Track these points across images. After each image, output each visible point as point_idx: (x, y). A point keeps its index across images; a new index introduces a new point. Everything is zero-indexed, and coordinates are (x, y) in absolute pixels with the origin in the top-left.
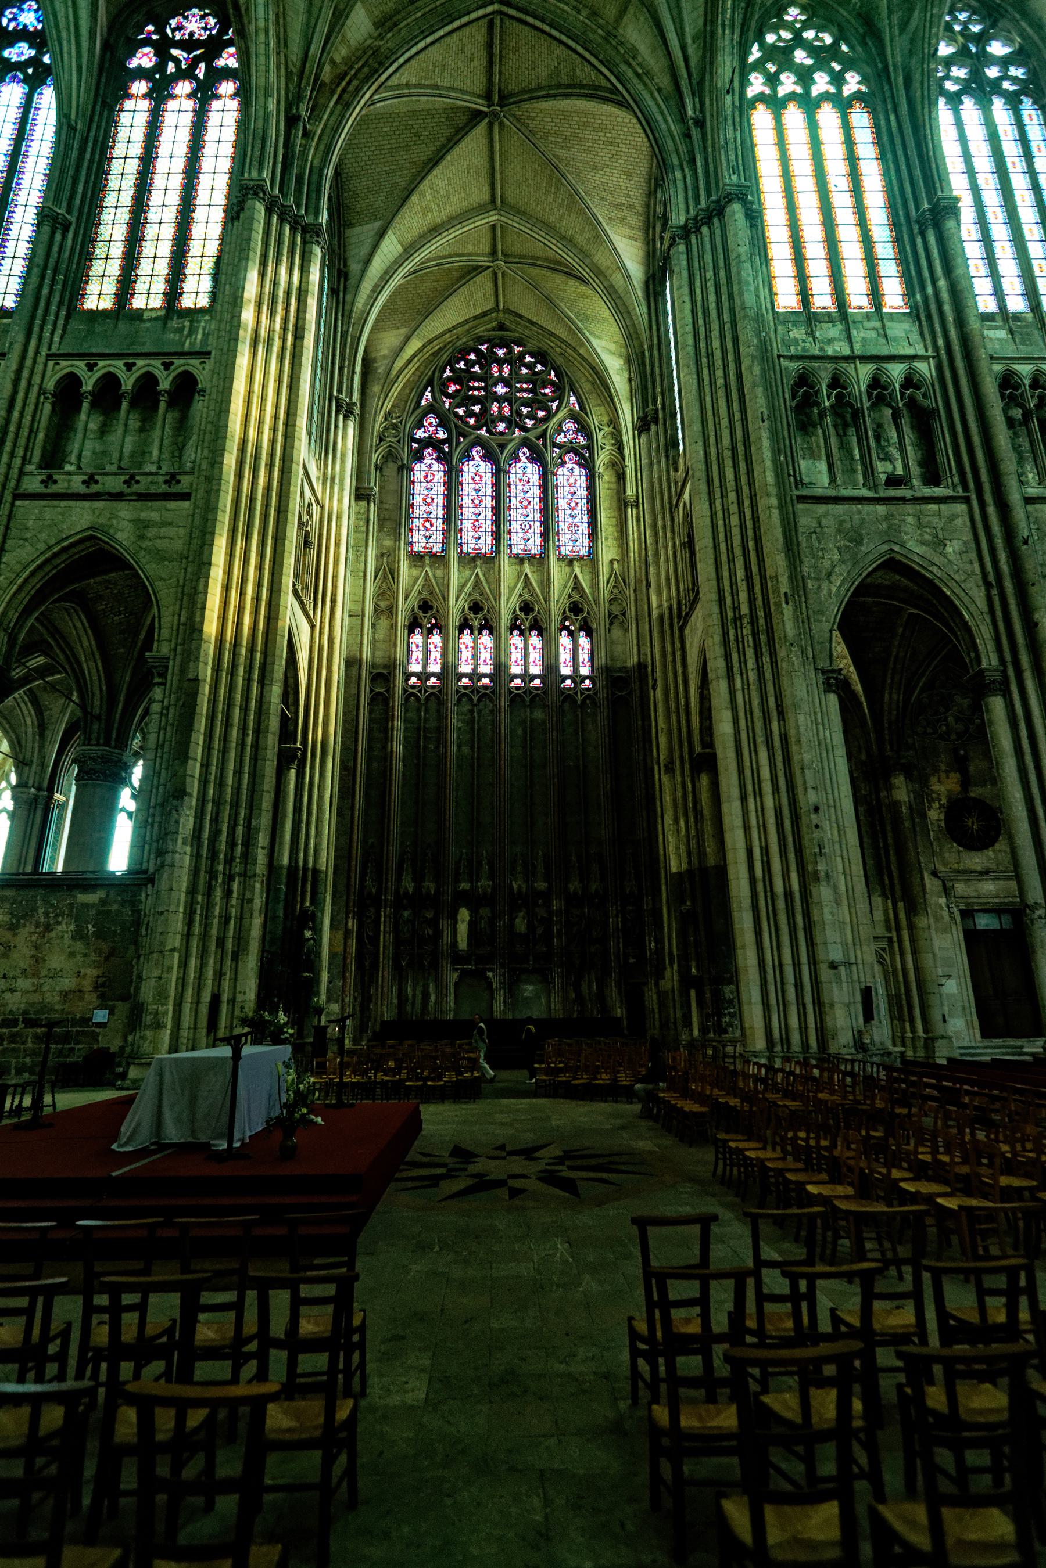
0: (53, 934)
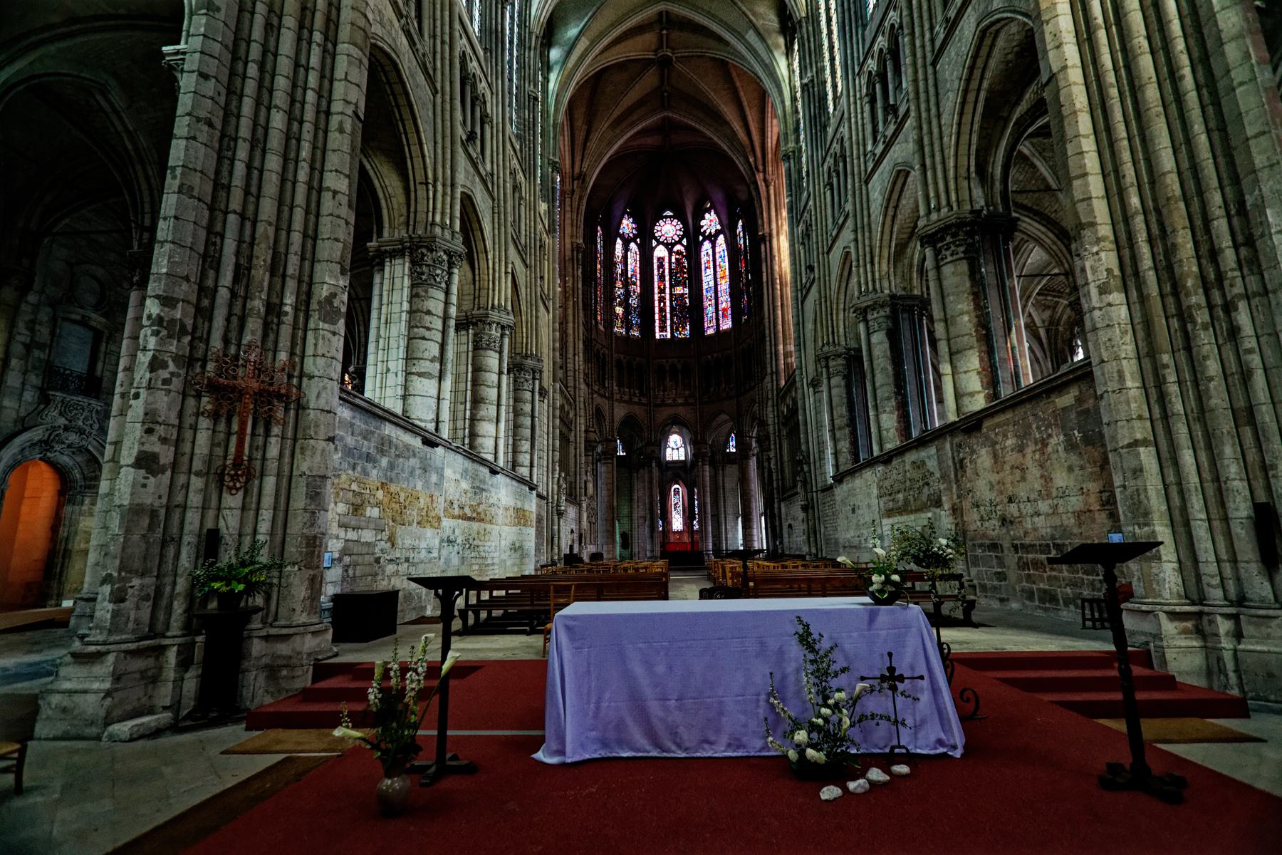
0: (1049, 449)
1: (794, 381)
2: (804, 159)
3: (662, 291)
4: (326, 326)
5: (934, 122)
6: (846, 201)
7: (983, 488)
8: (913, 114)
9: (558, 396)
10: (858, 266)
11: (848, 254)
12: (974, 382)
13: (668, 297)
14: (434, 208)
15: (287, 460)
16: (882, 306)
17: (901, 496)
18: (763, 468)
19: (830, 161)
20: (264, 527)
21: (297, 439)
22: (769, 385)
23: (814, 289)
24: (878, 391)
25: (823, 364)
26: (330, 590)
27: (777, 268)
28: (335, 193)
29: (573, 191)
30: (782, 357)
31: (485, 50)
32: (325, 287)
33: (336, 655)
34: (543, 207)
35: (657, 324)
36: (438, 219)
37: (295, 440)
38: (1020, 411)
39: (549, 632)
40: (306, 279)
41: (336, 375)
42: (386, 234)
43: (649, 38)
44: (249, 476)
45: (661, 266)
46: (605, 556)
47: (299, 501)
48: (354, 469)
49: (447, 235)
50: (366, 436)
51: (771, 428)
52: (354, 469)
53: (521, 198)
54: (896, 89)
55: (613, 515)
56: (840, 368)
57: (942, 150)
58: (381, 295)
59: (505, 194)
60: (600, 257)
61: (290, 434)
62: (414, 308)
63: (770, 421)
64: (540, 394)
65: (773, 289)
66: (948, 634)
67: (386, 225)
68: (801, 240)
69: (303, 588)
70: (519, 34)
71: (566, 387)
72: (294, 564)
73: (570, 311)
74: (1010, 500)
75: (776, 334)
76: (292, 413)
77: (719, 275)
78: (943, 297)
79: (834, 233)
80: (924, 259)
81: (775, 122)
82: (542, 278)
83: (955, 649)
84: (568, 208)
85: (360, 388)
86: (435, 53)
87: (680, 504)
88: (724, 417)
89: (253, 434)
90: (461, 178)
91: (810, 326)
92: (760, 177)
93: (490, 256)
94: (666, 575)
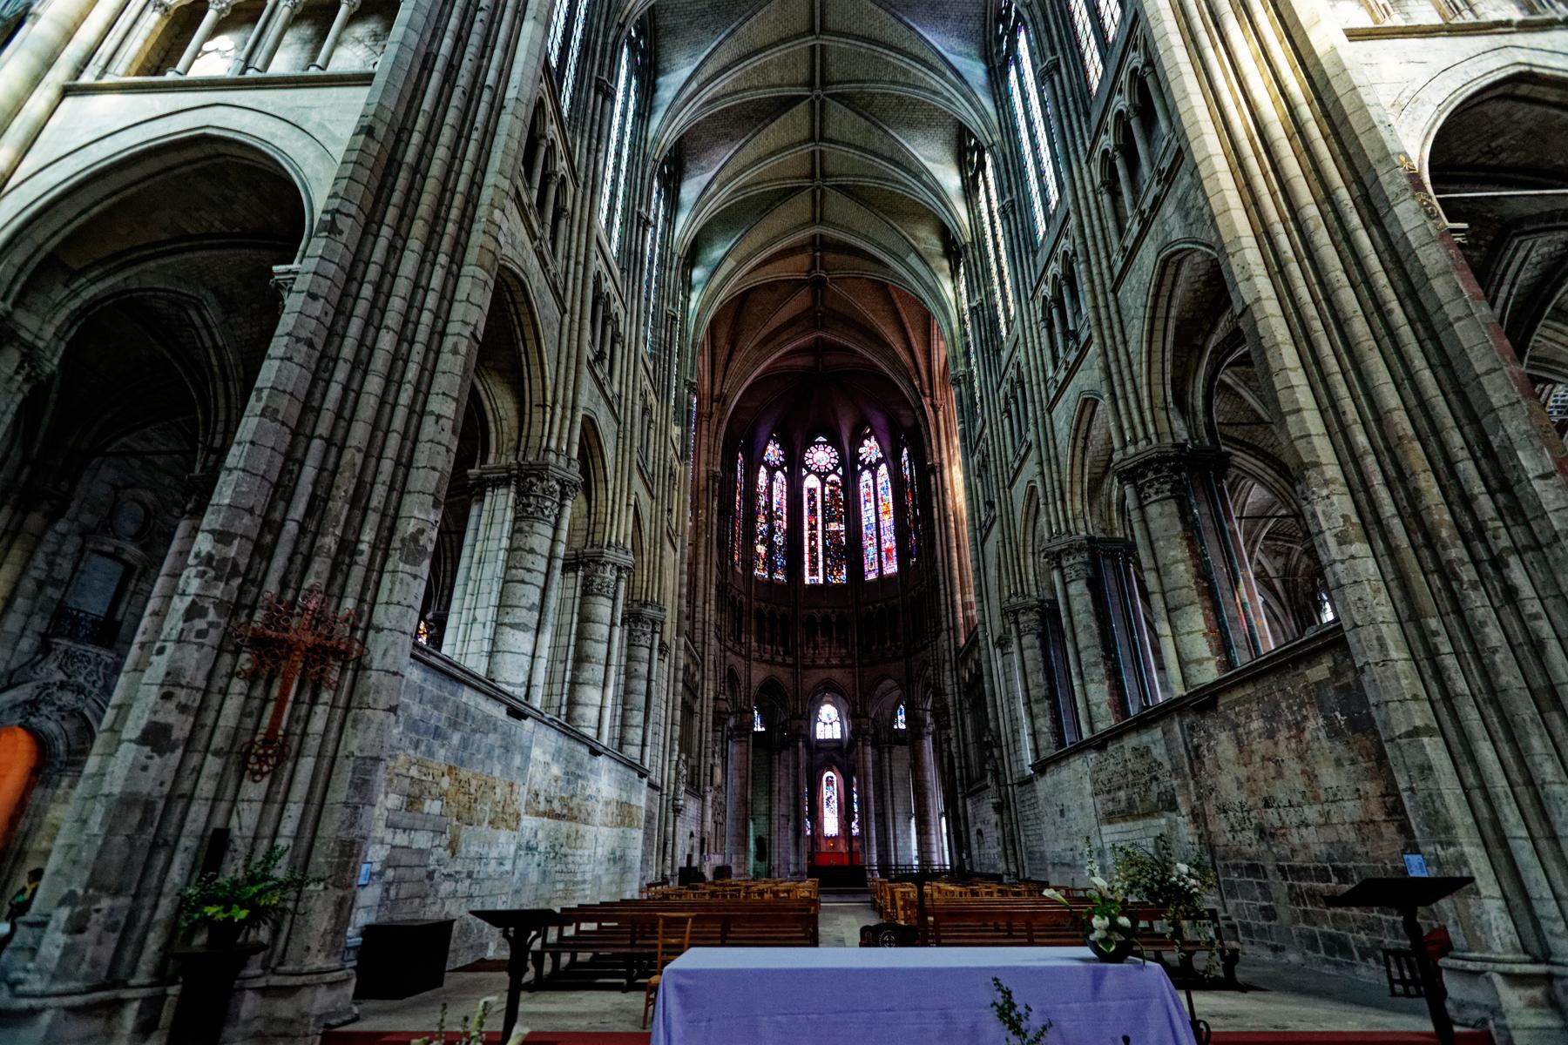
2: (976, 384)
3: (813, 527)
4: (408, 568)
5: (1121, 349)
6: (1028, 430)
7: (1228, 785)
8: (1096, 340)
9: (682, 654)
10: (1046, 504)
11: (1034, 488)
12: (1201, 647)
13: (820, 534)
15: (333, 735)
16: (1079, 550)
17: (1122, 794)
18: (942, 751)
19: (1006, 387)
20: (288, 827)
21: (349, 709)
23: (996, 527)
24: (1082, 655)
25: (1012, 618)
26: (361, 918)
27: (950, 503)
28: (439, 417)
30: (960, 609)
31: (622, 270)
32: (413, 521)
33: (356, 1019)
34: (676, 431)
35: (807, 566)
36: (553, 444)
37: (347, 708)
38: (1263, 685)
39: (655, 989)
40: (391, 512)
41: (410, 629)
42: (491, 460)
43: (802, 260)
44: (281, 757)
45: (812, 498)
46: (734, 871)
47: (341, 791)
48: (416, 748)
49: (562, 462)
50: (437, 704)
51: (950, 699)
52: (416, 748)
53: (651, 421)
54: (1075, 314)
55: (746, 813)
56: (1032, 624)
57: (1133, 379)
58: (477, 530)
59: (633, 417)
60: (740, 487)
61: (342, 702)
62: (515, 545)
63: (948, 690)
64: (660, 651)
66: (1204, 1002)
68: (978, 471)
69: (326, 917)
70: (660, 255)
71: (693, 643)
72: (319, 880)
73: (702, 550)
74: (1267, 805)
76: (349, 674)
77: (882, 509)
78: (1151, 543)
79: (1016, 465)
80: (1124, 497)
82: (670, 511)
83: (1217, 1025)
84: (704, 432)
85: (437, 641)
86: (567, 273)
87: (835, 798)
88: (889, 683)
89: (296, 701)
90: (583, 400)
91: (992, 572)
92: (926, 401)
93: (610, 486)
94: (815, 903)
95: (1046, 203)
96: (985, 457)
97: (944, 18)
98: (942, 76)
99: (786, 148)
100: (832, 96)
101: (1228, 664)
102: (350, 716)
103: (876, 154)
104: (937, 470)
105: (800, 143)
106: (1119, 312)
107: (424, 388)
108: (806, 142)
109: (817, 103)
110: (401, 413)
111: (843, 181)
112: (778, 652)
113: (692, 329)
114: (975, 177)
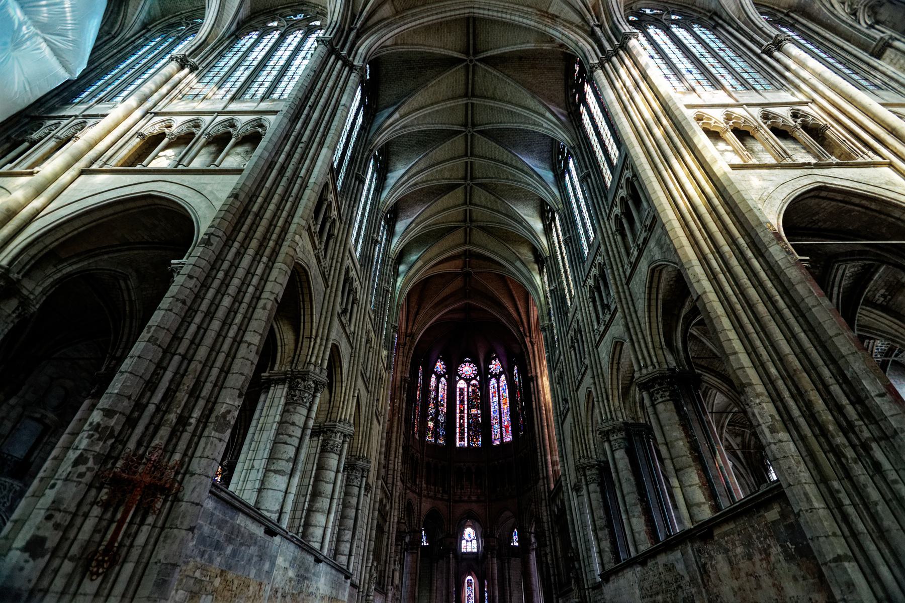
1: (561, 486)
2: (555, 331)
3: (462, 412)
5: (634, 315)
8: (620, 310)
9: (379, 491)
10: (598, 401)
11: (590, 392)
12: (699, 496)
13: (466, 416)
14: (312, 353)
15: (150, 547)
16: (620, 430)
19: (571, 333)
22: (542, 488)
23: (570, 414)
27: (542, 398)
28: (250, 344)
29: (405, 344)
30: (550, 465)
31: (361, 266)
32: (225, 406)
34: (385, 353)
35: (458, 436)
36: (313, 360)
37: (163, 528)
40: (213, 399)
43: (459, 262)
44: (113, 562)
45: (462, 394)
48: (202, 556)
49: (318, 371)
50: (221, 524)
51: (546, 525)
53: (370, 347)
57: (642, 332)
58: (262, 410)
60: (420, 386)
61: (160, 524)
62: (284, 420)
63: (545, 519)
64: (366, 489)
65: (541, 413)
67: (278, 362)
68: (557, 381)
71: (386, 484)
75: (544, 446)
76: (168, 504)
78: (661, 428)
79: (579, 378)
80: (643, 399)
81: (535, 308)
82: (378, 400)
84: (401, 354)
85: (227, 480)
86: (331, 266)
87: (473, 595)
88: (508, 513)
89: (131, 523)
90: (333, 335)
91: (569, 442)
92: (527, 340)
95: (588, 238)
96: (561, 373)
97: (532, 151)
98: (532, 177)
99: (452, 207)
100: (476, 184)
101: (716, 507)
102: (163, 534)
103: (498, 212)
104: (535, 379)
105: (459, 206)
106: (631, 295)
107: (243, 328)
108: (462, 205)
109: (468, 188)
110: (228, 341)
111: (482, 224)
112: (439, 491)
113: (397, 297)
114: (550, 224)
